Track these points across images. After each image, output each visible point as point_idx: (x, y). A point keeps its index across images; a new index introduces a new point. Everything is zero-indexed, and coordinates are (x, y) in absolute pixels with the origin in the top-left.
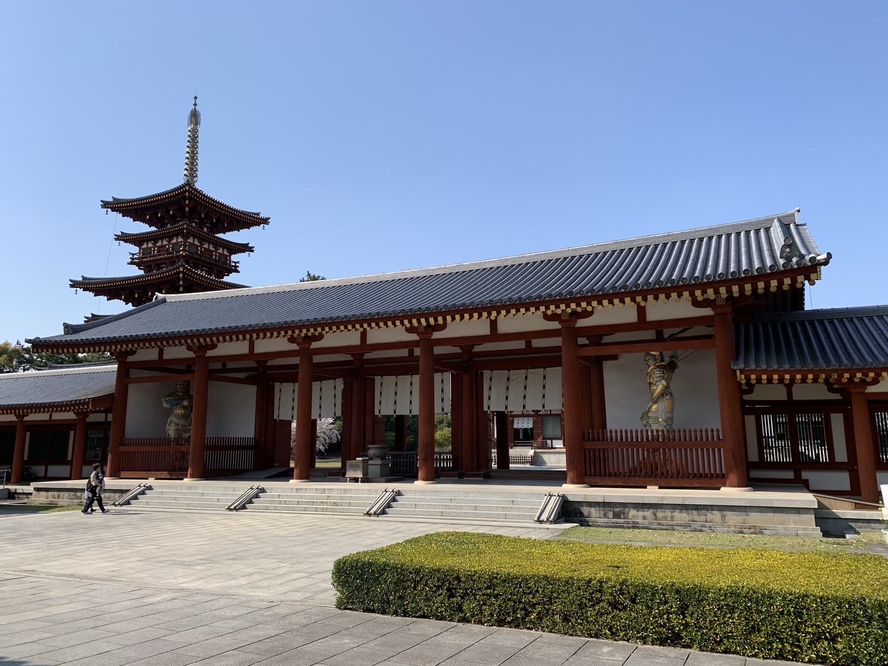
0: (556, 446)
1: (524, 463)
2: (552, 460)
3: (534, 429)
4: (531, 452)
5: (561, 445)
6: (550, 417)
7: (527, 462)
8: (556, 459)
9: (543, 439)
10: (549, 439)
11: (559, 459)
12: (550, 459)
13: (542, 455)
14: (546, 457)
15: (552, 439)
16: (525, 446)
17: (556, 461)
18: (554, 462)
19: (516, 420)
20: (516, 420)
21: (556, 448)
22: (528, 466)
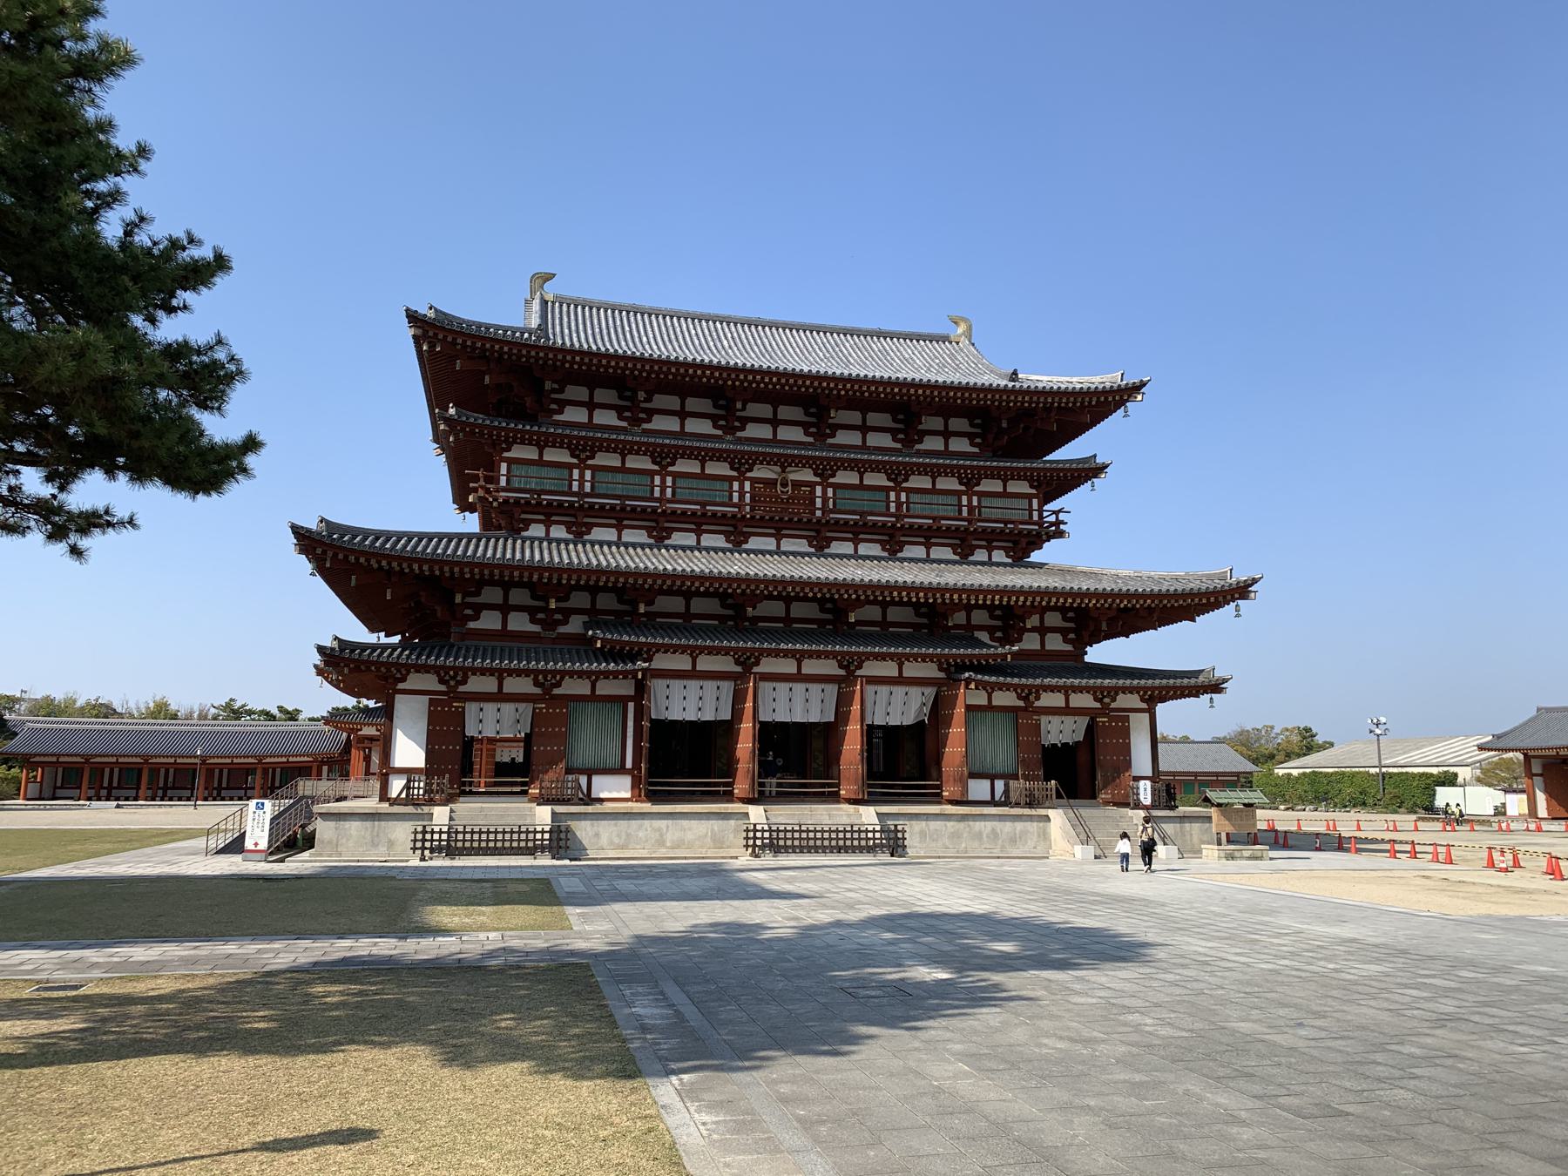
0: (602, 795)
1: (530, 852)
2: (604, 840)
3: (534, 738)
4: (543, 815)
5: (626, 791)
6: (590, 707)
7: (543, 849)
8: (619, 836)
9: (569, 771)
10: (581, 771)
11: (628, 835)
12: (597, 835)
13: (573, 824)
14: (584, 831)
15: (590, 773)
16: (498, 793)
17: (616, 841)
18: (611, 843)
19: (471, 709)
20: (471, 709)
21: (601, 800)
22: (545, 861)
